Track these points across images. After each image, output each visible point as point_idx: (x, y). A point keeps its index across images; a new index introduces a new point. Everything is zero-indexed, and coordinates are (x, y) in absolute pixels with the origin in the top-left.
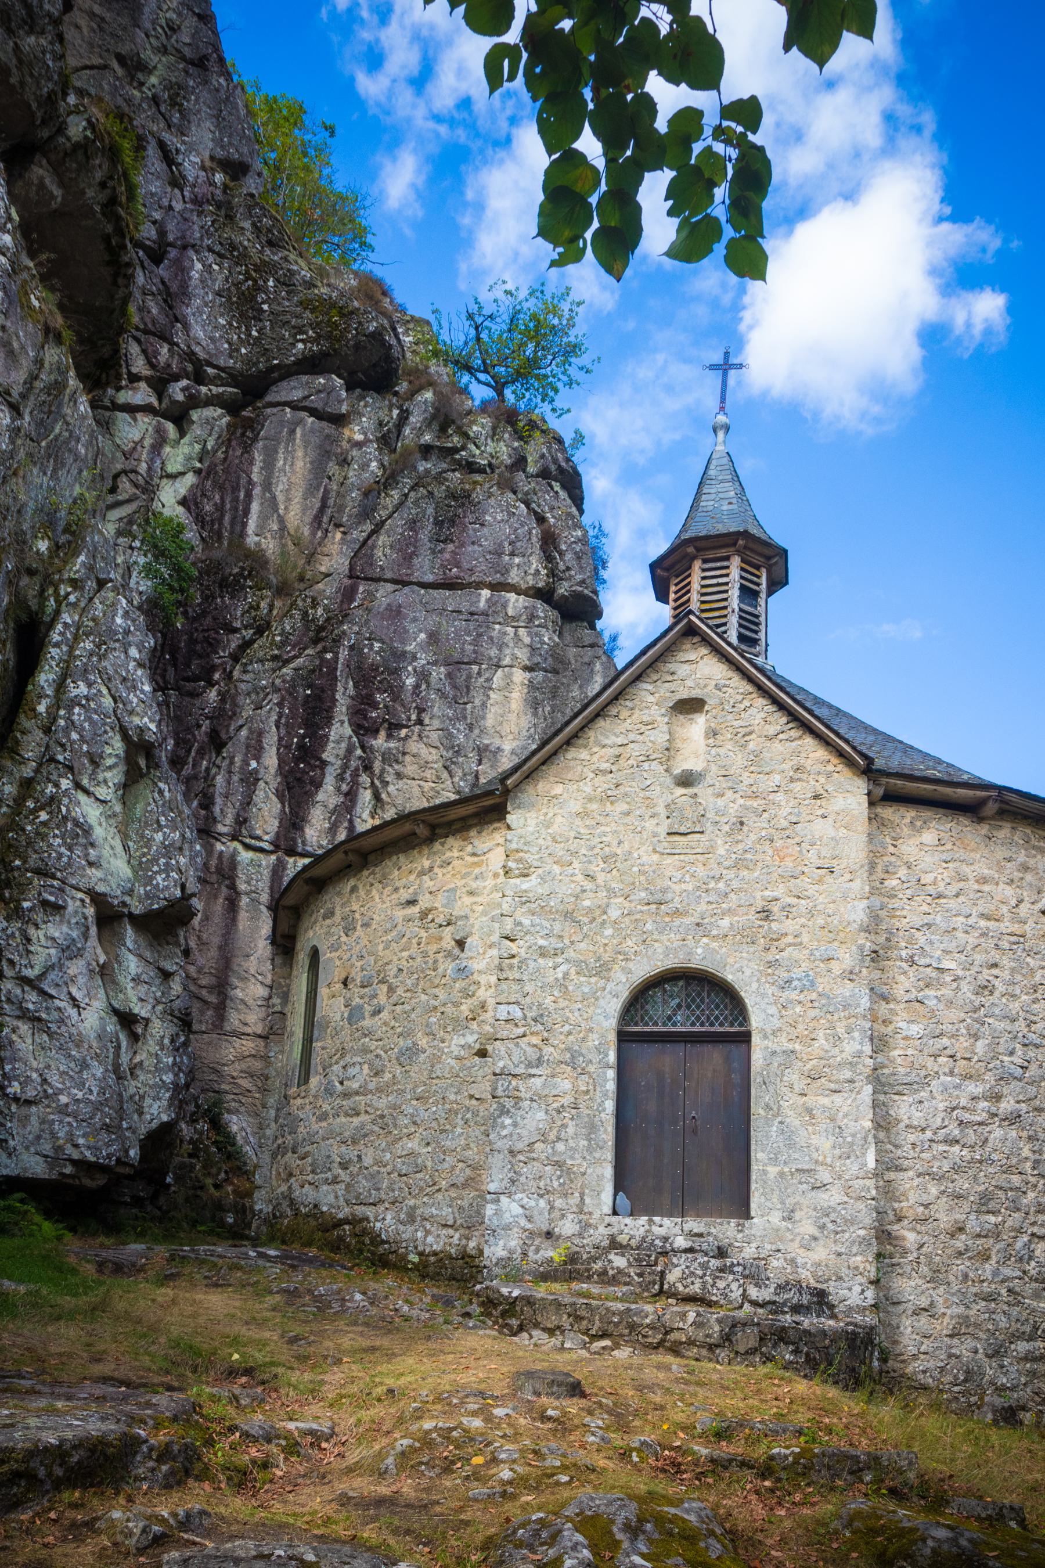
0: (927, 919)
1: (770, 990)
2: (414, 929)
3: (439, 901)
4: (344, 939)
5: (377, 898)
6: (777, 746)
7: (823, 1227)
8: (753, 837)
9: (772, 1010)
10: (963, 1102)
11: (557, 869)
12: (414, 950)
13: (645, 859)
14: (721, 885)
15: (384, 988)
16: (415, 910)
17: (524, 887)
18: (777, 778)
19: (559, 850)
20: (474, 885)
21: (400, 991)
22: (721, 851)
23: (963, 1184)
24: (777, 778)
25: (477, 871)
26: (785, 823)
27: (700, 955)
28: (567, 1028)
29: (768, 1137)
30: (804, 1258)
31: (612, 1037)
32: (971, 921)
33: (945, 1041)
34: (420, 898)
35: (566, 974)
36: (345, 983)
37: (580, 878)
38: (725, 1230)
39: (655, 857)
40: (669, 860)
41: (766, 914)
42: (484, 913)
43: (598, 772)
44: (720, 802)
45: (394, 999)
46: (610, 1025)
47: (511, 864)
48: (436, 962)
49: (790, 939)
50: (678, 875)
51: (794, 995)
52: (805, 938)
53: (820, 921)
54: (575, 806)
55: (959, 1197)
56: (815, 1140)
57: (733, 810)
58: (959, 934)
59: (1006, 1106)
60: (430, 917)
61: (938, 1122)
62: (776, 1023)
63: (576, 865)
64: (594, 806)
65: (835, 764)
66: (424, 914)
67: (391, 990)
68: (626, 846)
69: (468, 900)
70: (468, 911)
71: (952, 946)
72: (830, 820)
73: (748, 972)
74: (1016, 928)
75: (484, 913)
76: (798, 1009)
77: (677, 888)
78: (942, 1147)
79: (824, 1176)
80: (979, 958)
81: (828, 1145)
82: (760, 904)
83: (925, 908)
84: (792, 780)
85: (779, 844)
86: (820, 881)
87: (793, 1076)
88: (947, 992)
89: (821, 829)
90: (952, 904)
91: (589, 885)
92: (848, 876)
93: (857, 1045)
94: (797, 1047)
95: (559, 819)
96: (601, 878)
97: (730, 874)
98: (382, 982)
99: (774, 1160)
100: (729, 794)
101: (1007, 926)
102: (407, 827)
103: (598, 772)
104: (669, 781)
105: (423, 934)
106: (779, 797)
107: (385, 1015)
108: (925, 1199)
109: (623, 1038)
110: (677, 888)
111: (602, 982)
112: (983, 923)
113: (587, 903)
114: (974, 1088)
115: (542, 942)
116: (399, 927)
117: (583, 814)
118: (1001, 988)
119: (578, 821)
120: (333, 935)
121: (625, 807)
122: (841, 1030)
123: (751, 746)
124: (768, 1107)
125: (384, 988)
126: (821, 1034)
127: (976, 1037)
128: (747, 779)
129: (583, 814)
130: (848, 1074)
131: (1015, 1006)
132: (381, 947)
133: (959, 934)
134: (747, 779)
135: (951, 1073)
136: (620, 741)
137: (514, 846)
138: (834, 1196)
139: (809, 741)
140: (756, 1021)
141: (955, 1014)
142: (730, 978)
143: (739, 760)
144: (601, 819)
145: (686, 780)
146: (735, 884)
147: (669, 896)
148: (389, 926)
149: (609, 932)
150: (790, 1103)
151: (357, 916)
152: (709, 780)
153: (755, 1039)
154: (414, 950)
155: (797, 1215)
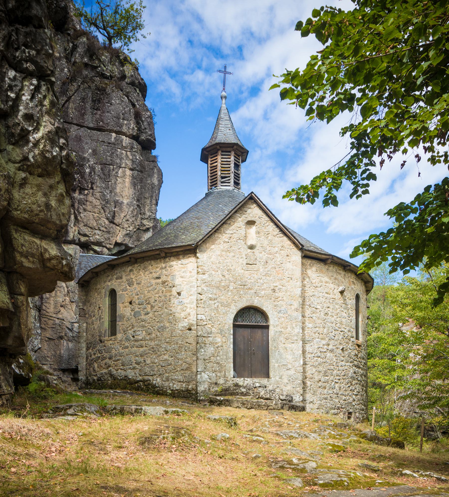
0: (314, 293)
1: (275, 313)
2: (160, 287)
3: (169, 279)
4: (128, 287)
5: (142, 274)
6: (276, 238)
7: (289, 380)
8: (270, 267)
9: (276, 319)
10: (321, 346)
11: (213, 273)
12: (160, 294)
13: (240, 271)
14: (261, 281)
15: (149, 306)
16: (160, 281)
17: (204, 278)
18: (276, 249)
19: (214, 267)
20: (183, 275)
21: (156, 307)
22: (261, 270)
23: (321, 369)
24: (276, 249)
25: (183, 270)
26: (279, 263)
27: (256, 302)
28: (219, 323)
29: (275, 355)
30: (285, 389)
31: (232, 326)
32: (324, 294)
33: (317, 329)
34: (162, 277)
35: (218, 306)
36: (131, 303)
37: (221, 276)
38: (264, 381)
39: (243, 271)
40: (247, 272)
41: (274, 290)
42: (187, 284)
43: (225, 242)
44: (261, 255)
45: (154, 310)
46: (232, 321)
47: (199, 270)
48: (170, 299)
49: (280, 298)
50: (249, 277)
51: (282, 315)
52: (285, 298)
53: (289, 294)
54: (218, 253)
55: (320, 372)
56: (287, 356)
57: (264, 258)
58: (321, 298)
59: (330, 347)
60: (166, 284)
61: (315, 352)
62: (277, 323)
63: (219, 272)
64: (224, 253)
65: (292, 246)
66: (164, 283)
67: (152, 307)
68: (234, 267)
69: (181, 279)
70: (180, 283)
71: (319, 302)
72: (291, 263)
73: (269, 308)
74: (333, 297)
75: (187, 284)
76: (283, 319)
77: (249, 281)
78: (316, 358)
79: (290, 366)
80: (325, 305)
81: (291, 358)
82: (272, 288)
83: (313, 290)
84: (281, 250)
85: (277, 269)
86: (289, 282)
87: (282, 339)
88: (318, 315)
89: (289, 266)
90: (319, 289)
91: (223, 279)
92: (296, 281)
93: (298, 330)
94: (283, 330)
95: (213, 257)
96: (227, 276)
97: (264, 278)
98: (148, 304)
99: (277, 362)
100: (263, 252)
101: (331, 296)
102: (157, 252)
103: (225, 242)
104: (246, 247)
105: (164, 289)
106: (277, 255)
107: (150, 315)
108: (312, 372)
109: (235, 326)
110: (249, 281)
111: (228, 309)
112: (326, 295)
113: (223, 284)
114: (324, 342)
115: (210, 296)
116: (154, 286)
117: (221, 256)
118: (330, 314)
119: (219, 257)
120: (123, 285)
121: (233, 254)
122: (294, 326)
123: (269, 238)
124: (275, 347)
125: (149, 306)
126: (289, 326)
127: (324, 328)
128: (268, 248)
129: (221, 256)
130: (296, 338)
131: (333, 319)
132: (146, 292)
133: (321, 298)
134: (268, 248)
135: (318, 338)
136: (231, 232)
137: (200, 264)
138: (292, 372)
139: (285, 238)
140: (272, 322)
141: (320, 321)
142: (264, 309)
143: (266, 242)
144: (226, 257)
145: (252, 247)
146: (265, 281)
147: (247, 283)
148: (149, 285)
149: (230, 293)
150: (281, 346)
151: (134, 280)
152: (257, 248)
153: (271, 328)
154: (160, 294)
155: (283, 377)
